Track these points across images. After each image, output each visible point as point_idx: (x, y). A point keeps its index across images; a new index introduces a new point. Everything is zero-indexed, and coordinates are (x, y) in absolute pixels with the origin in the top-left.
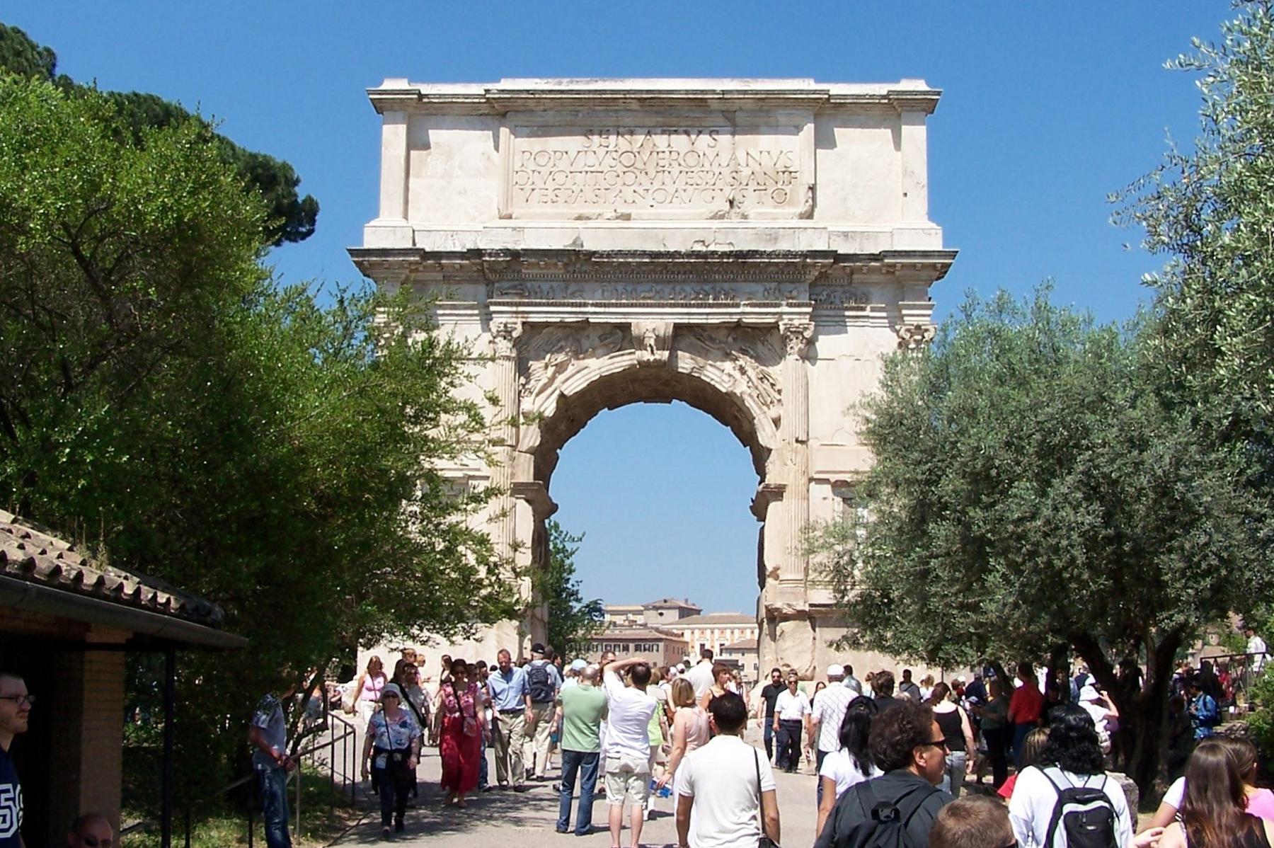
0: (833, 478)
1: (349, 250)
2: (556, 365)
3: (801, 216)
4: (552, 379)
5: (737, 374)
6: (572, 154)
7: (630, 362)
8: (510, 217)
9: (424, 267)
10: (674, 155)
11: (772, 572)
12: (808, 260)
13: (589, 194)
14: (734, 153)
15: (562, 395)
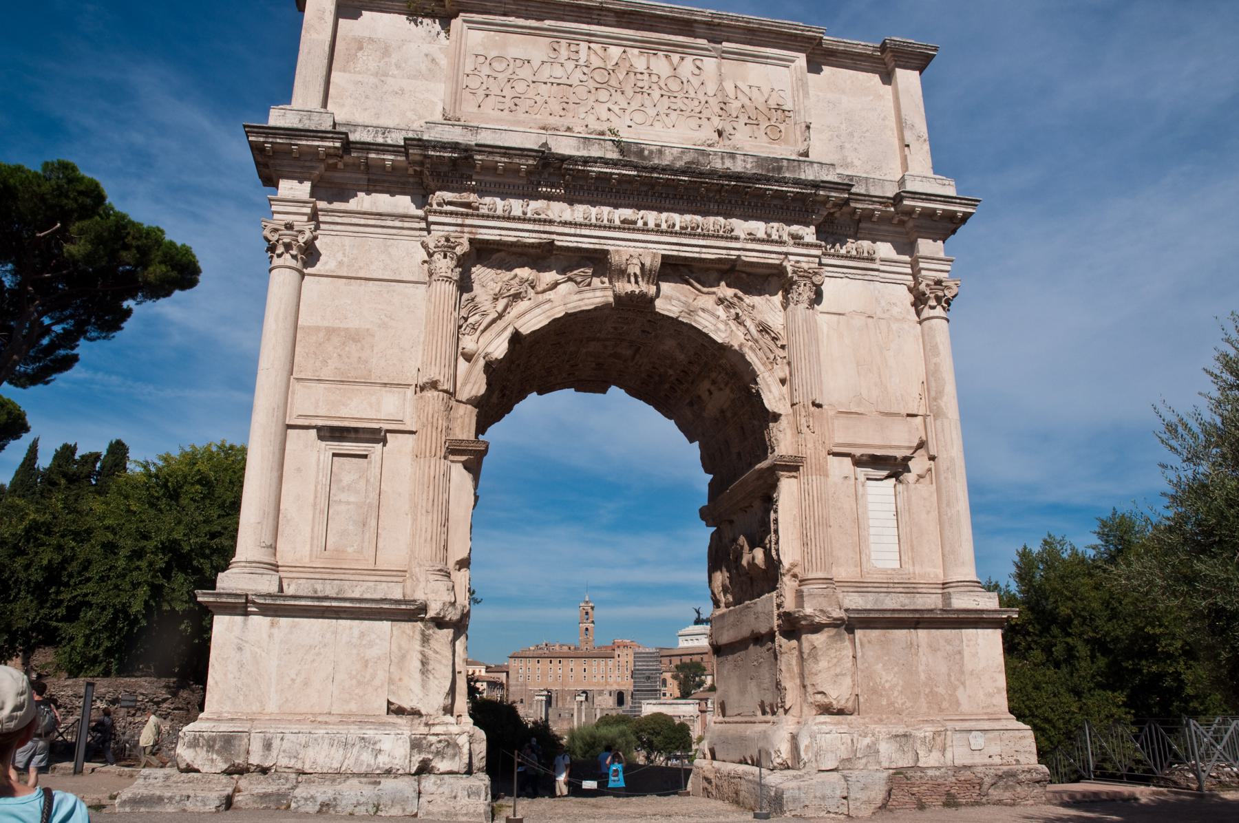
0: (858, 452)
1: (245, 126)
2: (509, 296)
3: (801, 155)
4: (500, 316)
5: (733, 324)
6: (536, 63)
7: (602, 300)
8: (459, 120)
9: (346, 165)
10: (655, 79)
11: (789, 571)
12: (821, 193)
13: (555, 106)
14: (721, 83)
15: (516, 338)
